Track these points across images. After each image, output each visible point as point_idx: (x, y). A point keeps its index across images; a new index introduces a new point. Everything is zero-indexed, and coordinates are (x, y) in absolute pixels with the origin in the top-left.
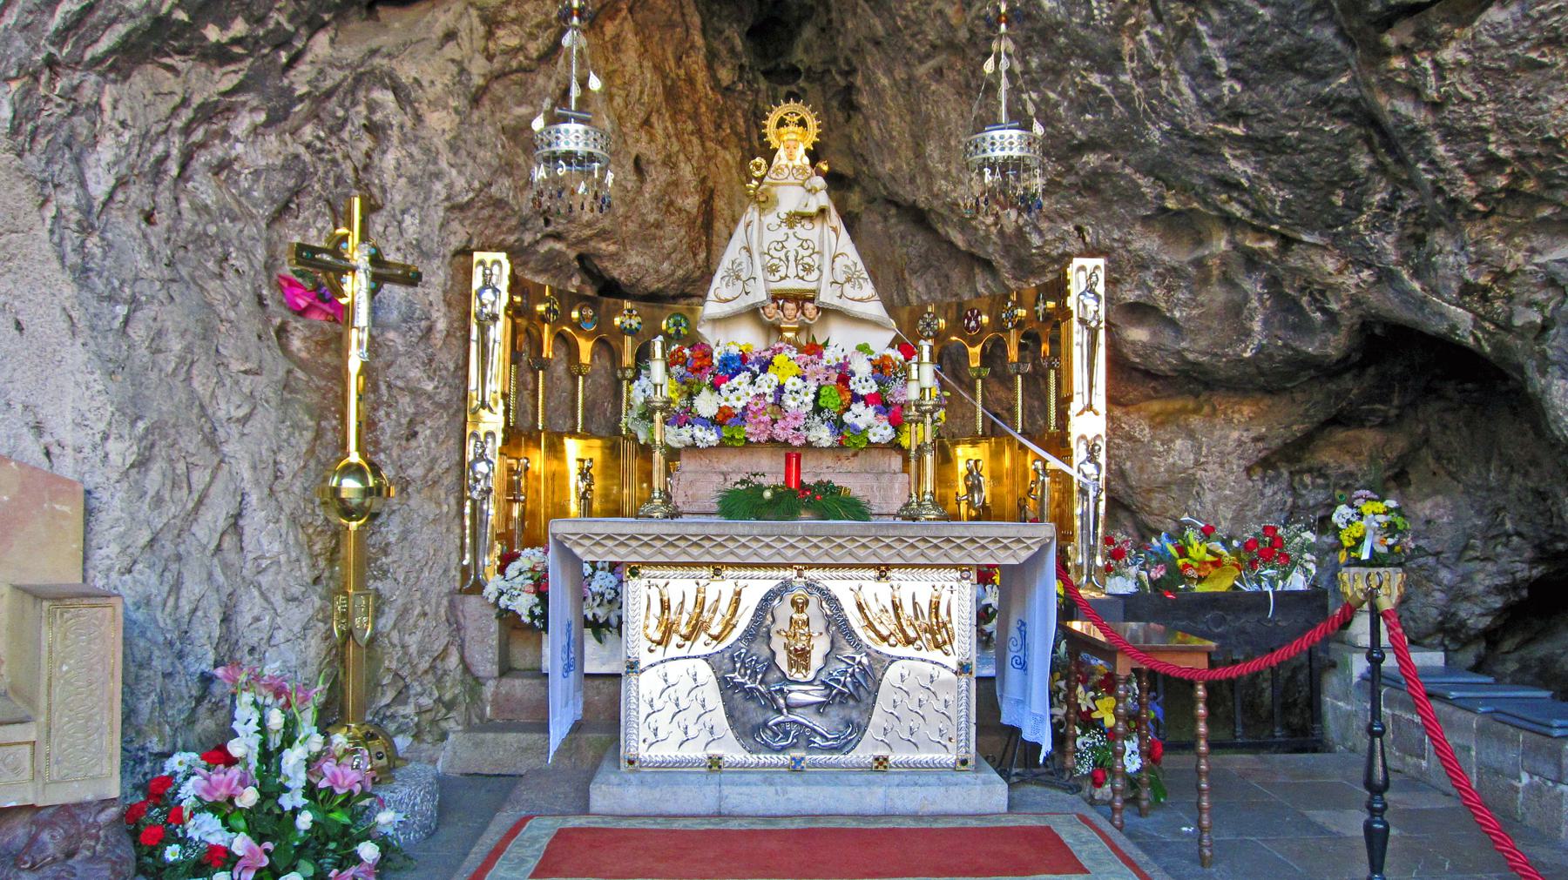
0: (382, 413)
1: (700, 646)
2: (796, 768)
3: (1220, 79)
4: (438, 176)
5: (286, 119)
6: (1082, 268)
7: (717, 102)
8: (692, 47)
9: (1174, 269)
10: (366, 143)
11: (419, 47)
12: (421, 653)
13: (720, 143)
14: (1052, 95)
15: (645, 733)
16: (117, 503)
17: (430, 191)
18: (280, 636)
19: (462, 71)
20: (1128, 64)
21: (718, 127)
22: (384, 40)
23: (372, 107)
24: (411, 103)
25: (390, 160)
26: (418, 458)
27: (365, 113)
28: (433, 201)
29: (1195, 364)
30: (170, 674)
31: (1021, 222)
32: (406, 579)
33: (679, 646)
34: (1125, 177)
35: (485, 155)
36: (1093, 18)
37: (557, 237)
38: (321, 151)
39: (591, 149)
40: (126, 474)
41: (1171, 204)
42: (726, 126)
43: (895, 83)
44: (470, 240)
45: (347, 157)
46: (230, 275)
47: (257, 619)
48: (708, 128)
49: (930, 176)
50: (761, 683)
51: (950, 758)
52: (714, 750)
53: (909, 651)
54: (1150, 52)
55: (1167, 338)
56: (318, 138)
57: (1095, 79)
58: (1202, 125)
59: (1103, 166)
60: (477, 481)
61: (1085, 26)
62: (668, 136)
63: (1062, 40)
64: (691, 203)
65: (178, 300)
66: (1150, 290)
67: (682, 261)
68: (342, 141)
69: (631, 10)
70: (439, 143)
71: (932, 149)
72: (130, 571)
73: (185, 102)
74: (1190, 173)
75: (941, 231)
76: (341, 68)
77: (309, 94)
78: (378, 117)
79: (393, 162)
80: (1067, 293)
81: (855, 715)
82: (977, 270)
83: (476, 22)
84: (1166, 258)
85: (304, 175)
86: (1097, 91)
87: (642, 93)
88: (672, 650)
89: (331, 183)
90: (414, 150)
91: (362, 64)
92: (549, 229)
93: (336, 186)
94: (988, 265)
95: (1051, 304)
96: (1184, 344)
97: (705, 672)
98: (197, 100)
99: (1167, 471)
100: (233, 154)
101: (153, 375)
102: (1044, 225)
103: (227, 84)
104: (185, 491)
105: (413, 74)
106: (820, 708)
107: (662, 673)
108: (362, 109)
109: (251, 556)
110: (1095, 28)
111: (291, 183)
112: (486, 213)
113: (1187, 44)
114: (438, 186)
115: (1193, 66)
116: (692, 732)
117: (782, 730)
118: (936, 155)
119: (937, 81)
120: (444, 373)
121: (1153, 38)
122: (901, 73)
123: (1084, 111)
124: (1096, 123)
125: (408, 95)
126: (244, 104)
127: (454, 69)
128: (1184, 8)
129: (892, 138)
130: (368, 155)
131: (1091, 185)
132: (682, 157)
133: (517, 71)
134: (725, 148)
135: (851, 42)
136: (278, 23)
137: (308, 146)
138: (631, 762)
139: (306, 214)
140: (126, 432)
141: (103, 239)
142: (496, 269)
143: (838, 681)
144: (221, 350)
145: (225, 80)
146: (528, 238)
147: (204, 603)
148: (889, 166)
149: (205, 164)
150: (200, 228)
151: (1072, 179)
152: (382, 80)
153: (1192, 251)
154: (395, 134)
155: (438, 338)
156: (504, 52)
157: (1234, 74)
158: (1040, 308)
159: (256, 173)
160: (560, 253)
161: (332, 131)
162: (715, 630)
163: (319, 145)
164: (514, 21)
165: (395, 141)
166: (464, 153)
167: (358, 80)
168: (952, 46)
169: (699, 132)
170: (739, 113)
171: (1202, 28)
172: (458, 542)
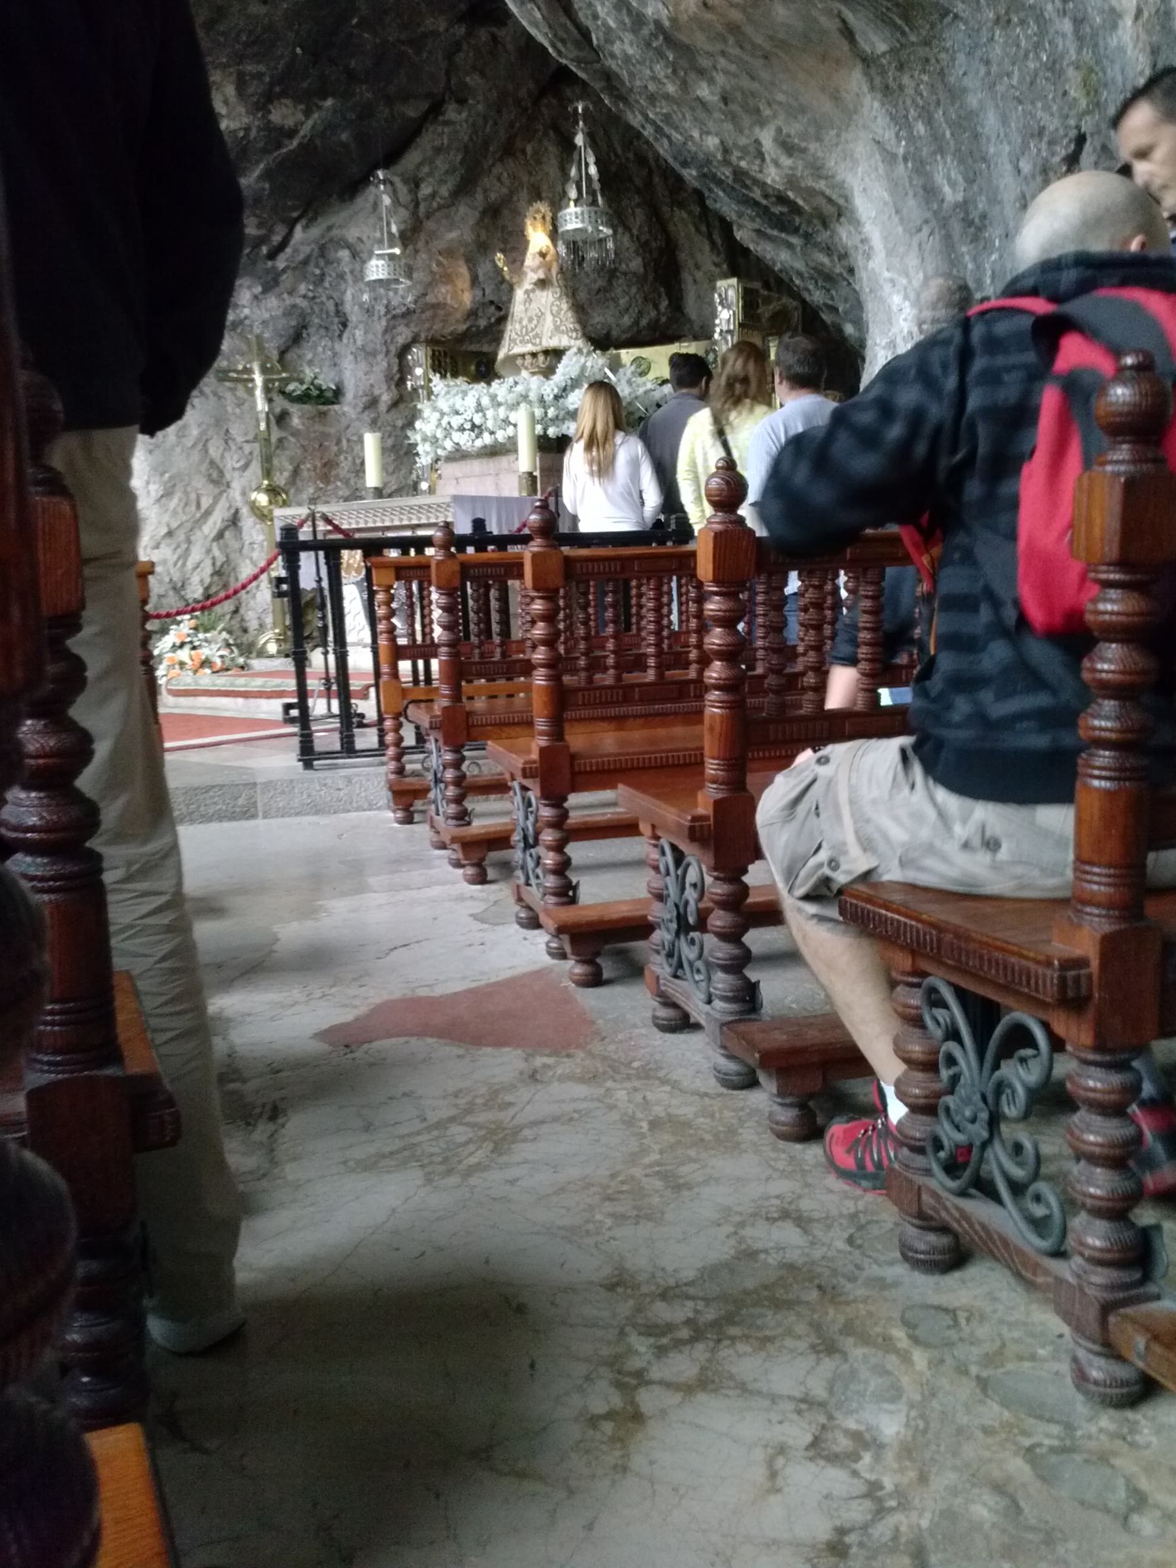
0: (342, 458)
16: (153, 515)
24: (358, 254)
30: (163, 596)
38: (314, 298)
40: (158, 500)
68: (325, 288)
76: (309, 244)
77: (287, 267)
85: (303, 315)
100: (242, 316)
101: (178, 450)
104: (193, 508)
111: (294, 323)
112: (428, 314)
120: (389, 428)
137: (304, 297)
139: (314, 338)
146: (482, 323)
154: (349, 277)
159: (264, 323)
161: (316, 285)
163: (311, 294)
165: (350, 282)
167: (323, 250)
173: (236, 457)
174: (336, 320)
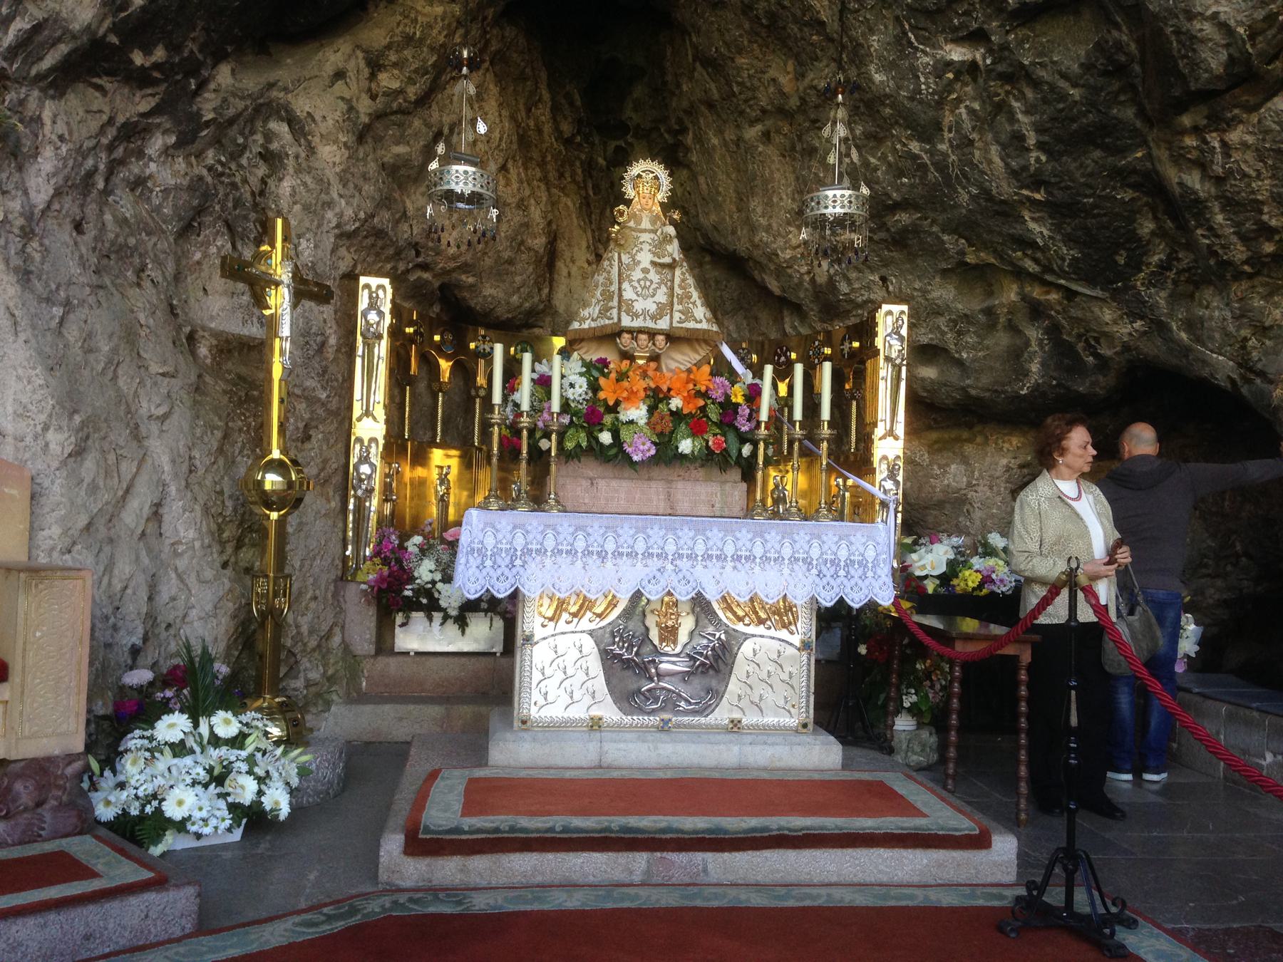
1: (586, 623)
2: (664, 728)
3: (1028, 150)
4: (329, 204)
5: (193, 142)
6: (890, 313)
7: (560, 152)
8: (540, 100)
9: (966, 315)
10: (262, 170)
11: (313, 83)
12: (311, 632)
13: (562, 189)
14: (872, 160)
15: (536, 696)
16: (56, 488)
17: (323, 217)
18: (193, 613)
19: (351, 109)
20: (946, 134)
21: (561, 176)
22: (283, 74)
23: (269, 136)
24: (305, 135)
25: (287, 185)
26: (312, 459)
27: (261, 141)
28: (325, 228)
29: (977, 399)
31: (832, 271)
32: (302, 566)
33: (568, 623)
34: (931, 234)
35: (368, 188)
36: (920, 93)
37: (425, 267)
38: (222, 174)
39: (478, 189)
40: (64, 463)
41: (970, 259)
42: (567, 175)
43: (725, 144)
44: (355, 266)
45: (245, 181)
46: (147, 284)
47: (173, 599)
48: (552, 175)
49: (753, 229)
50: (637, 654)
51: (793, 722)
52: (596, 712)
53: (761, 630)
54: (967, 124)
55: (954, 375)
56: (219, 162)
57: (915, 147)
58: (1005, 188)
59: (914, 224)
60: (361, 481)
61: (912, 99)
62: (521, 182)
63: (888, 111)
64: (539, 243)
65: (105, 305)
66: (943, 334)
67: (530, 296)
68: (240, 166)
69: (492, 63)
70: (330, 174)
71: (756, 205)
72: (69, 552)
73: (111, 121)
74: (991, 232)
75: (757, 277)
76: (242, 98)
77: (214, 120)
78: (274, 146)
79: (288, 189)
80: (876, 334)
81: (714, 683)
82: (786, 313)
83: (362, 64)
84: (960, 306)
86: (917, 157)
87: (501, 139)
88: (562, 626)
89: (230, 205)
90: (308, 180)
91: (262, 95)
92: (420, 260)
93: (235, 208)
94: (797, 309)
95: (856, 344)
96: (968, 382)
97: (589, 645)
98: (121, 119)
99: (942, 491)
100: (148, 172)
102: (853, 275)
103: (144, 107)
104: (116, 480)
105: (307, 109)
106: (685, 677)
107: (552, 645)
108: (259, 138)
109: (168, 542)
110: (921, 102)
111: (195, 203)
112: (369, 241)
113: (1001, 119)
114: (330, 215)
115: (1003, 137)
116: (576, 697)
117: (651, 695)
118: (759, 210)
119: (763, 143)
121: (971, 111)
122: (730, 135)
123: (901, 174)
124: (912, 186)
125: (302, 128)
126: (159, 125)
127: (344, 107)
128: (1002, 86)
129: (718, 193)
130: (263, 182)
131: (900, 241)
132: (532, 201)
133: (395, 113)
134: (567, 195)
135: (685, 104)
136: (192, 52)
137: (210, 169)
138: (524, 722)
139: (207, 232)
140: (65, 423)
141: (41, 245)
142: (381, 293)
143: (701, 654)
144: (142, 353)
145: (143, 102)
147: (132, 584)
148: (713, 217)
149: (123, 180)
150: (121, 240)
151: (882, 235)
152: (278, 112)
153: (983, 301)
154: (290, 163)
155: (330, 353)
156: (385, 94)
157: (1041, 146)
158: (846, 346)
159: (166, 191)
160: (427, 281)
162: (599, 610)
164: (395, 65)
165: (291, 170)
166: (351, 185)
167: (257, 110)
168: (782, 112)
169: (545, 179)
170: (578, 164)
171: (1016, 104)
172: (340, 534)
173: (157, 400)
174: (253, 216)
